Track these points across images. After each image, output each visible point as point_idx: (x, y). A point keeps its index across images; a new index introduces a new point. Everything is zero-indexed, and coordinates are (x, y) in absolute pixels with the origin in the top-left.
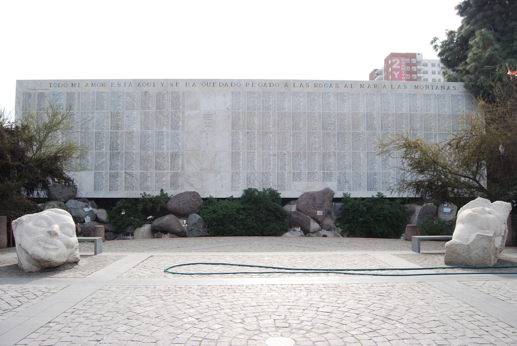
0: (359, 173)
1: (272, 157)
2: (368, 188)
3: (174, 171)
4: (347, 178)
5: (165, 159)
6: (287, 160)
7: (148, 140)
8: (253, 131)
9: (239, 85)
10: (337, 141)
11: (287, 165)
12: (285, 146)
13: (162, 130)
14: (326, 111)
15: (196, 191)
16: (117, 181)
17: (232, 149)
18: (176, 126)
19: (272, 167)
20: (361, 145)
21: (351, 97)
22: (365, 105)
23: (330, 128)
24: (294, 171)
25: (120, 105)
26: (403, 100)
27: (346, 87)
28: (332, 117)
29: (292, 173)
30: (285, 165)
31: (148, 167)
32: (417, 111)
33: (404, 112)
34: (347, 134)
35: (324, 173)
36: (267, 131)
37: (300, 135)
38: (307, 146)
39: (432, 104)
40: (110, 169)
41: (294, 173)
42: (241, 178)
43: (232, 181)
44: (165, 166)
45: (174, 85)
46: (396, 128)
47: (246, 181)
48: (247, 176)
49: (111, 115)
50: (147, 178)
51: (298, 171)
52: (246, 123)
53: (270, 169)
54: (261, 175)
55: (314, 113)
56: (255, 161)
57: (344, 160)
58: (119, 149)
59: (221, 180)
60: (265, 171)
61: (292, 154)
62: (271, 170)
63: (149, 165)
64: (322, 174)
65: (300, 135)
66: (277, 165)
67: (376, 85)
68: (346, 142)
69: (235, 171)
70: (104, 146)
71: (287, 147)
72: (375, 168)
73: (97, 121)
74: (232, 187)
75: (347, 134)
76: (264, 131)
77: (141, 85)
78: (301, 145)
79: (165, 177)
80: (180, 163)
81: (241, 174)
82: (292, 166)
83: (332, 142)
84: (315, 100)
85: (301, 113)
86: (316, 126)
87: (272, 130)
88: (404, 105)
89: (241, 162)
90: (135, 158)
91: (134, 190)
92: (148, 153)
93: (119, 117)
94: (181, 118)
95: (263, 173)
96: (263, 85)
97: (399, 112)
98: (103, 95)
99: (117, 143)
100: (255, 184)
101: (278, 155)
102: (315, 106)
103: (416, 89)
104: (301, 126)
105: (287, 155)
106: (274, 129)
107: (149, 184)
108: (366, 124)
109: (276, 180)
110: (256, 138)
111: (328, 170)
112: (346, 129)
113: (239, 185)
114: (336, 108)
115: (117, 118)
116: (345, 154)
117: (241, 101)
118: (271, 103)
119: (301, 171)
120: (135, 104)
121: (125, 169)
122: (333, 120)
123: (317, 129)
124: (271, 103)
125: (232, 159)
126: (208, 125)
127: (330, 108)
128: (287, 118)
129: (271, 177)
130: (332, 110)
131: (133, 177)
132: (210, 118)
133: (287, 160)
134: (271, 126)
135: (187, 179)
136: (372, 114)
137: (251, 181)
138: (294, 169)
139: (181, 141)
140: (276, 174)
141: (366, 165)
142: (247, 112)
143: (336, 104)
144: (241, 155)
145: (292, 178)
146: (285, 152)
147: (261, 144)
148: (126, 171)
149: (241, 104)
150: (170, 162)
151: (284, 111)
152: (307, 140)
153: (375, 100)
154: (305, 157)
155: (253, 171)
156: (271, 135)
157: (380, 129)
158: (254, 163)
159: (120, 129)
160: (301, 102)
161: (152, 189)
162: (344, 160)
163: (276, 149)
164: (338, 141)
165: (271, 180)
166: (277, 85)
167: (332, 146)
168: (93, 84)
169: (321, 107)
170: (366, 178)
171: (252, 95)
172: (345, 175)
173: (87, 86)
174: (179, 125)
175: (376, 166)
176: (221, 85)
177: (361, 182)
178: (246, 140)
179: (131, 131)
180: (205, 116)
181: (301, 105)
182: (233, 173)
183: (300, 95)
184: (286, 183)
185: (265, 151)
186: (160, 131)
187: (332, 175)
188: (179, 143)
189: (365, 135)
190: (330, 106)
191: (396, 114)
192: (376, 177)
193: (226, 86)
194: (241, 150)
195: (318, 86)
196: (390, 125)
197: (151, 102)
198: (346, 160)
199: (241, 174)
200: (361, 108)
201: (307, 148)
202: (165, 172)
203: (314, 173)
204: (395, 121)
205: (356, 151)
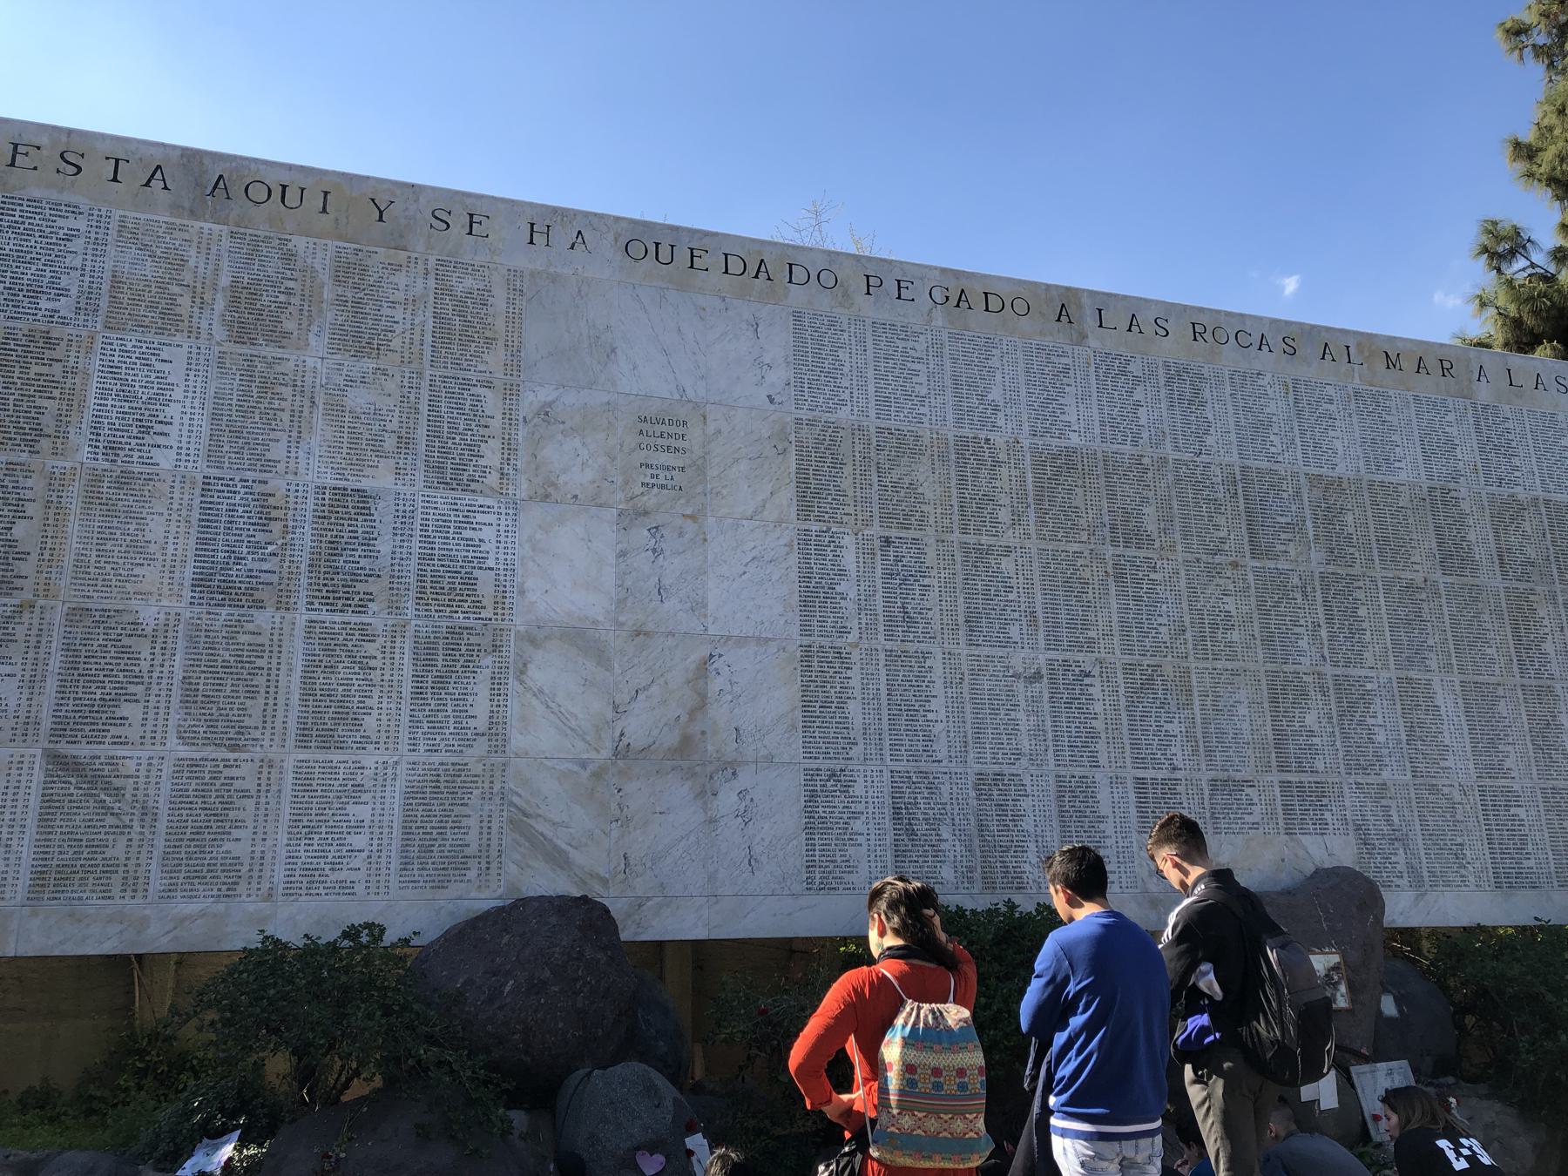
0: (1446, 790)
1: (1020, 686)
3: (436, 759)
4: (1396, 819)
5: (375, 676)
6: (1098, 707)
7: (260, 537)
8: (911, 534)
9: (827, 279)
11: (1103, 735)
12: (1086, 625)
13: (365, 484)
17: (806, 630)
18: (460, 468)
19: (1026, 745)
20: (1431, 642)
21: (1353, 406)
22: (1419, 450)
23: (1283, 548)
24: (1141, 773)
25: (63, 293)
28: (1285, 495)
29: (1130, 784)
30: (1093, 735)
31: (247, 722)
34: (1360, 584)
35: (1285, 785)
36: (984, 539)
37: (1153, 576)
38: (1188, 635)
41: (1140, 782)
42: (860, 807)
43: (809, 829)
44: (370, 722)
45: (459, 223)
47: (888, 824)
48: (896, 792)
50: (227, 805)
52: (876, 487)
53: (1018, 754)
54: (973, 794)
55: (1207, 465)
56: (934, 705)
57: (1370, 721)
58: (18, 583)
59: (745, 816)
61: (1120, 675)
62: (1024, 762)
63: (255, 707)
64: (1277, 790)
65: (1153, 576)
66: (1050, 735)
68: (1365, 625)
69: (823, 764)
71: (1092, 634)
75: (1360, 584)
76: (971, 539)
77: (237, 190)
78: (1163, 629)
79: (365, 797)
80: (481, 706)
81: (861, 780)
83: (1302, 622)
84: (1203, 403)
85: (1146, 461)
86: (1222, 534)
87: (1010, 538)
89: (853, 708)
90: (146, 654)
91: (116, 890)
92: (250, 627)
93: (45, 370)
94: (496, 424)
100: (944, 846)
101: (1053, 681)
102: (1207, 432)
104: (1151, 527)
105: (1097, 681)
106: (1019, 531)
107: (240, 849)
109: (1055, 823)
110: (934, 573)
113: (851, 851)
115: (35, 369)
116: (1369, 686)
117: (846, 370)
118: (995, 394)
119: (1178, 774)
120: (185, 301)
121: (60, 730)
122: (1294, 508)
123: (1226, 547)
124: (995, 394)
125: (805, 689)
126: (662, 481)
127: (1273, 449)
128: (1080, 483)
129: (1026, 804)
130: (1280, 459)
131: (118, 793)
132: (673, 443)
133: (1098, 707)
134: (1004, 515)
135: (525, 814)
136: (1453, 494)
137: (921, 828)
138: (1139, 762)
139: (491, 563)
140: (1052, 788)
141: (1468, 749)
142: (880, 430)
143: (1297, 432)
144: (856, 668)
145: (1133, 810)
146: (1085, 660)
147: (961, 608)
148: (64, 748)
149: (845, 383)
150: (407, 688)
152: (1185, 605)
153: (1453, 431)
155: (923, 766)
156: (1007, 565)
157: (1497, 568)
158: (930, 716)
159: (45, 444)
160: (1138, 405)
161: (265, 886)
162: (1370, 721)
163: (1042, 643)
164: (1330, 620)
165: (1027, 824)
166: (1020, 307)
167: (1303, 644)
169: (1233, 437)
170: (1480, 813)
171: (901, 344)
172: (1384, 802)
174: (482, 462)
175: (1512, 755)
177: (1459, 840)
178: (879, 582)
179: (137, 469)
180: (645, 427)
181: (1143, 421)
182: (811, 775)
183: (1130, 368)
184: (1109, 842)
185: (986, 651)
186: (350, 485)
187: (1325, 801)
188: (477, 573)
189: (1437, 594)
190: (1272, 438)
191: (1547, 502)
192: (1522, 812)
193: (763, 275)
194: (852, 637)
196: (1531, 552)
197: (296, 300)
198: (1380, 721)
199: (861, 780)
200: (1402, 465)
201: (1190, 646)
202: (370, 760)
204: (1549, 536)
205: (1413, 674)
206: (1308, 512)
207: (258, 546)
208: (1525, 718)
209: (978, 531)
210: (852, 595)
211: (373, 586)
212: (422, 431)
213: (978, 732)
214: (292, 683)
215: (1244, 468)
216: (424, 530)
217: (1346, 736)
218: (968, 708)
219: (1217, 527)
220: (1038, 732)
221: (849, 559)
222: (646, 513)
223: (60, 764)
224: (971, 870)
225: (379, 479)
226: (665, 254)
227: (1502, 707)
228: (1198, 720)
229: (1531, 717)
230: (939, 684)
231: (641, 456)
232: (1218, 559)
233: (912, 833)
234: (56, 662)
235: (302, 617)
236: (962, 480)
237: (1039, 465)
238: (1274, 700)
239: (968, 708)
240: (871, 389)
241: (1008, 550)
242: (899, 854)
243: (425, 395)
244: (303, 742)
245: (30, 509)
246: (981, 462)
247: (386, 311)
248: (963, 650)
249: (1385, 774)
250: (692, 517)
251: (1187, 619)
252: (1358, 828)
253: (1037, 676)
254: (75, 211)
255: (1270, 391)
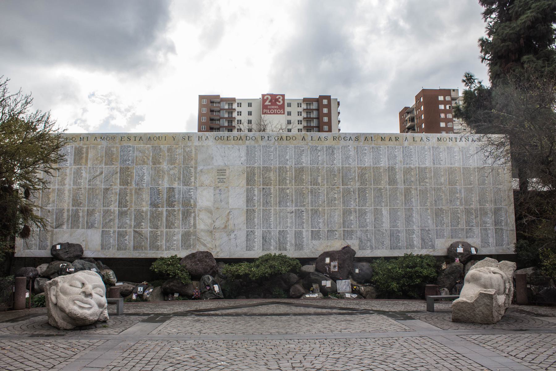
2: (391, 247)
3: (186, 230)
4: (369, 236)
5: (176, 217)
6: (305, 217)
7: (159, 196)
9: (254, 138)
10: (357, 197)
12: (303, 202)
13: (173, 186)
14: (346, 166)
15: (208, 251)
16: (126, 240)
17: (247, 206)
18: (188, 182)
19: (289, 225)
20: (383, 200)
21: (371, 150)
24: (312, 229)
25: (129, 160)
26: (426, 153)
27: (366, 140)
29: (310, 232)
30: (303, 223)
32: (441, 164)
33: (427, 165)
35: (344, 231)
38: (326, 203)
39: (456, 157)
40: (118, 228)
41: (312, 231)
44: (176, 225)
46: (419, 183)
47: (261, 240)
48: (263, 234)
49: (120, 170)
50: (157, 237)
51: (316, 230)
53: (287, 227)
56: (271, 218)
57: (366, 217)
59: (236, 239)
60: (282, 230)
62: (289, 228)
63: (159, 223)
67: (397, 138)
68: (368, 198)
70: (113, 203)
72: (398, 225)
73: (105, 177)
74: (247, 247)
76: (281, 187)
77: (152, 139)
80: (192, 222)
82: (310, 223)
85: (320, 168)
87: (289, 186)
88: (427, 158)
94: (193, 174)
95: (280, 231)
96: (279, 139)
97: (422, 166)
98: (112, 149)
99: (126, 200)
101: (296, 212)
102: (334, 160)
103: (439, 142)
104: (320, 181)
106: (291, 184)
107: (159, 244)
108: (387, 179)
111: (348, 227)
112: (367, 184)
113: (254, 244)
114: (356, 163)
118: (288, 157)
120: (146, 159)
124: (288, 157)
125: (247, 217)
129: (288, 236)
131: (142, 236)
132: (223, 174)
133: (305, 217)
134: (288, 182)
137: (267, 240)
138: (312, 227)
140: (294, 233)
142: (263, 167)
145: (310, 236)
146: (303, 209)
147: (278, 200)
148: (135, 229)
149: (256, 159)
150: (181, 219)
151: (301, 166)
152: (325, 197)
153: (397, 153)
154: (325, 214)
155: (269, 229)
156: (288, 191)
159: (129, 185)
160: (319, 156)
163: (294, 206)
164: (359, 197)
165: (288, 239)
166: (294, 138)
167: (352, 203)
168: (103, 138)
169: (341, 161)
173: (96, 140)
175: (400, 223)
176: (236, 138)
178: (262, 196)
180: (218, 171)
181: (320, 159)
182: (247, 232)
186: (171, 187)
189: (387, 190)
191: (419, 168)
192: (400, 235)
194: (256, 207)
195: (337, 139)
196: (413, 179)
198: (368, 217)
202: (176, 230)
203: (334, 231)
205: (378, 207)
206: (357, 175)
207: (158, 198)
208: (404, 215)
209: (282, 185)
210: (256, 199)
211: (175, 203)
212: (182, 176)
213: (280, 223)
214: (164, 219)
215: (342, 167)
216: (183, 193)
217: (359, 221)
218: (278, 218)
219: (335, 180)
220: (292, 223)
221: (256, 193)
222: (218, 187)
223: (135, 232)
224: (277, 247)
225: (175, 185)
226: (222, 139)
227: (399, 213)
228: (326, 219)
229: (406, 215)
230: (272, 215)
231: (217, 177)
232: (334, 187)
233: (266, 241)
234: (133, 217)
235: (165, 209)
236: (279, 175)
237: (296, 171)
238: (344, 214)
239: (278, 218)
240: (262, 159)
241: (288, 188)
242: (263, 245)
243: (182, 170)
244: (166, 228)
245: (128, 195)
246: (284, 171)
247: (176, 156)
248: (278, 208)
249: (368, 228)
250: (227, 187)
251: (326, 199)
252: (360, 238)
253: (292, 212)
254: (130, 147)
255: (351, 149)
